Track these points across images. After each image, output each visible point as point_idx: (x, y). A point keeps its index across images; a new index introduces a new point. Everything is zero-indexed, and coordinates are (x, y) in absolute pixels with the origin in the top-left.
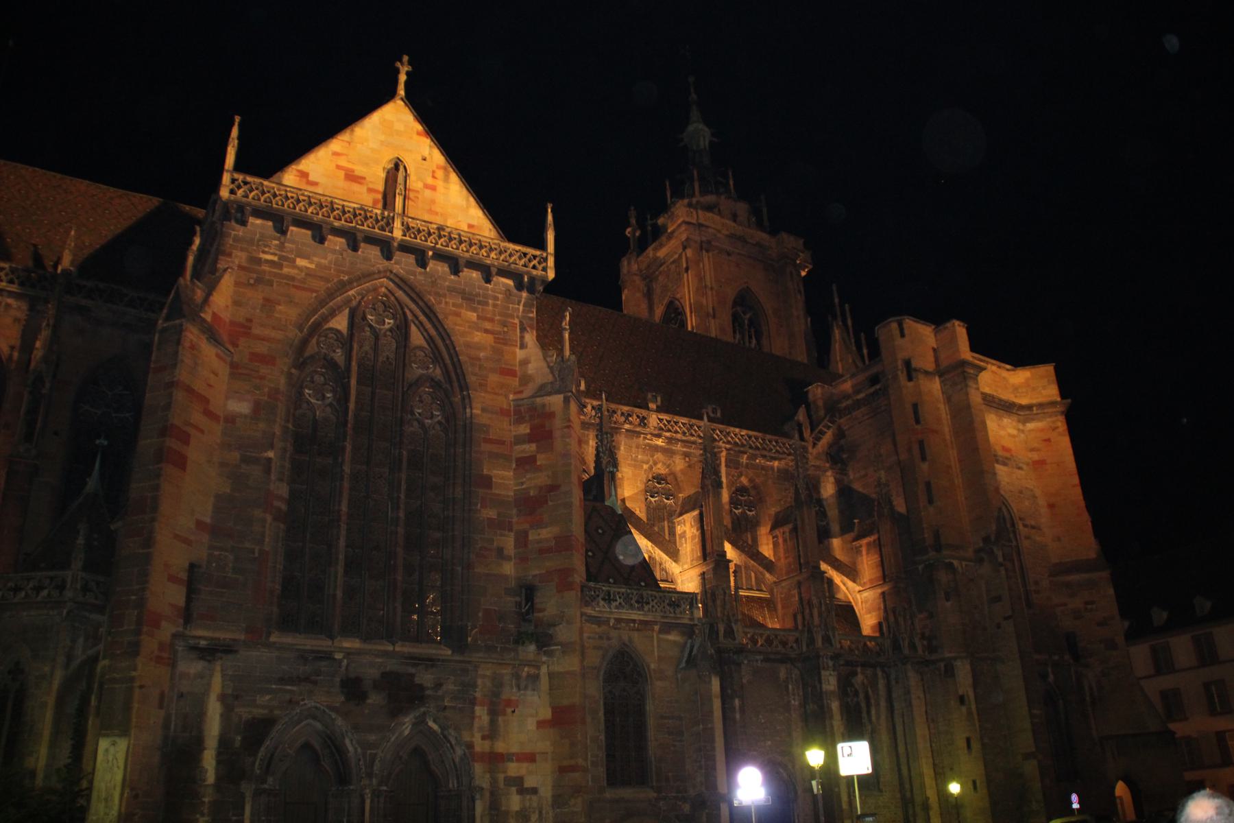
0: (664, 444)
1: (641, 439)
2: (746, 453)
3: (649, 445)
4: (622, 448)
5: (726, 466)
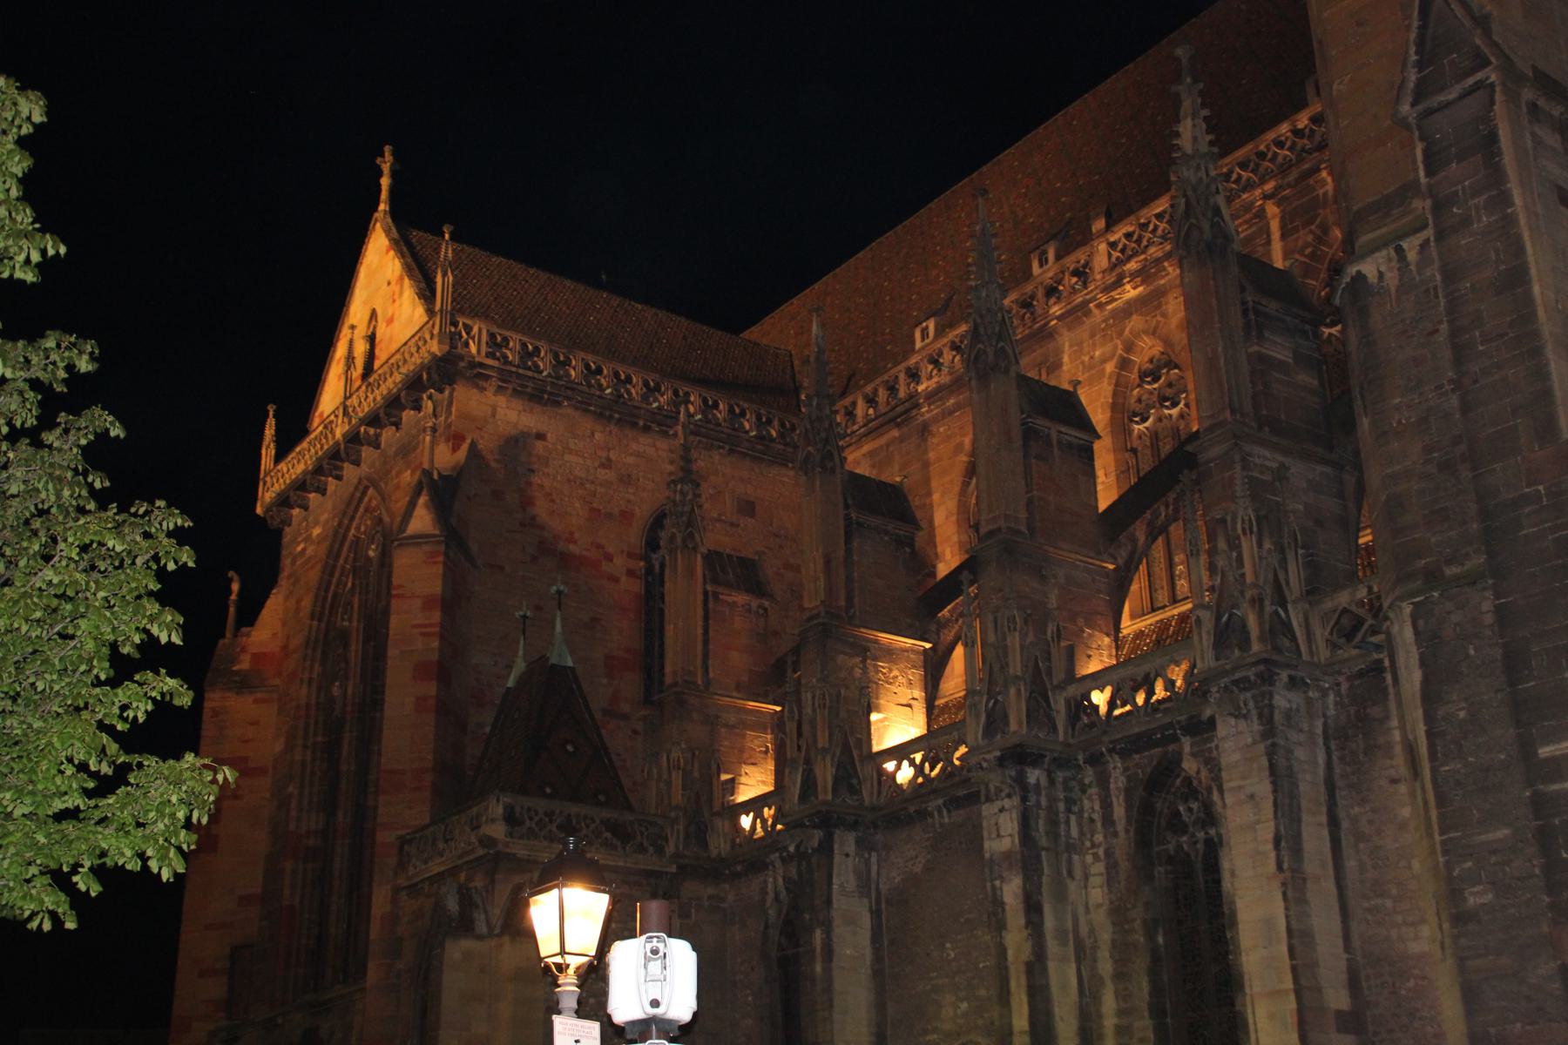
0: (1141, 289)
1: (1096, 311)
2: (1318, 170)
3: (1115, 314)
4: (1066, 359)
5: (1283, 237)
